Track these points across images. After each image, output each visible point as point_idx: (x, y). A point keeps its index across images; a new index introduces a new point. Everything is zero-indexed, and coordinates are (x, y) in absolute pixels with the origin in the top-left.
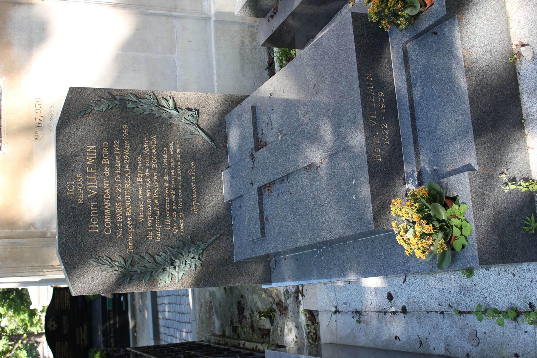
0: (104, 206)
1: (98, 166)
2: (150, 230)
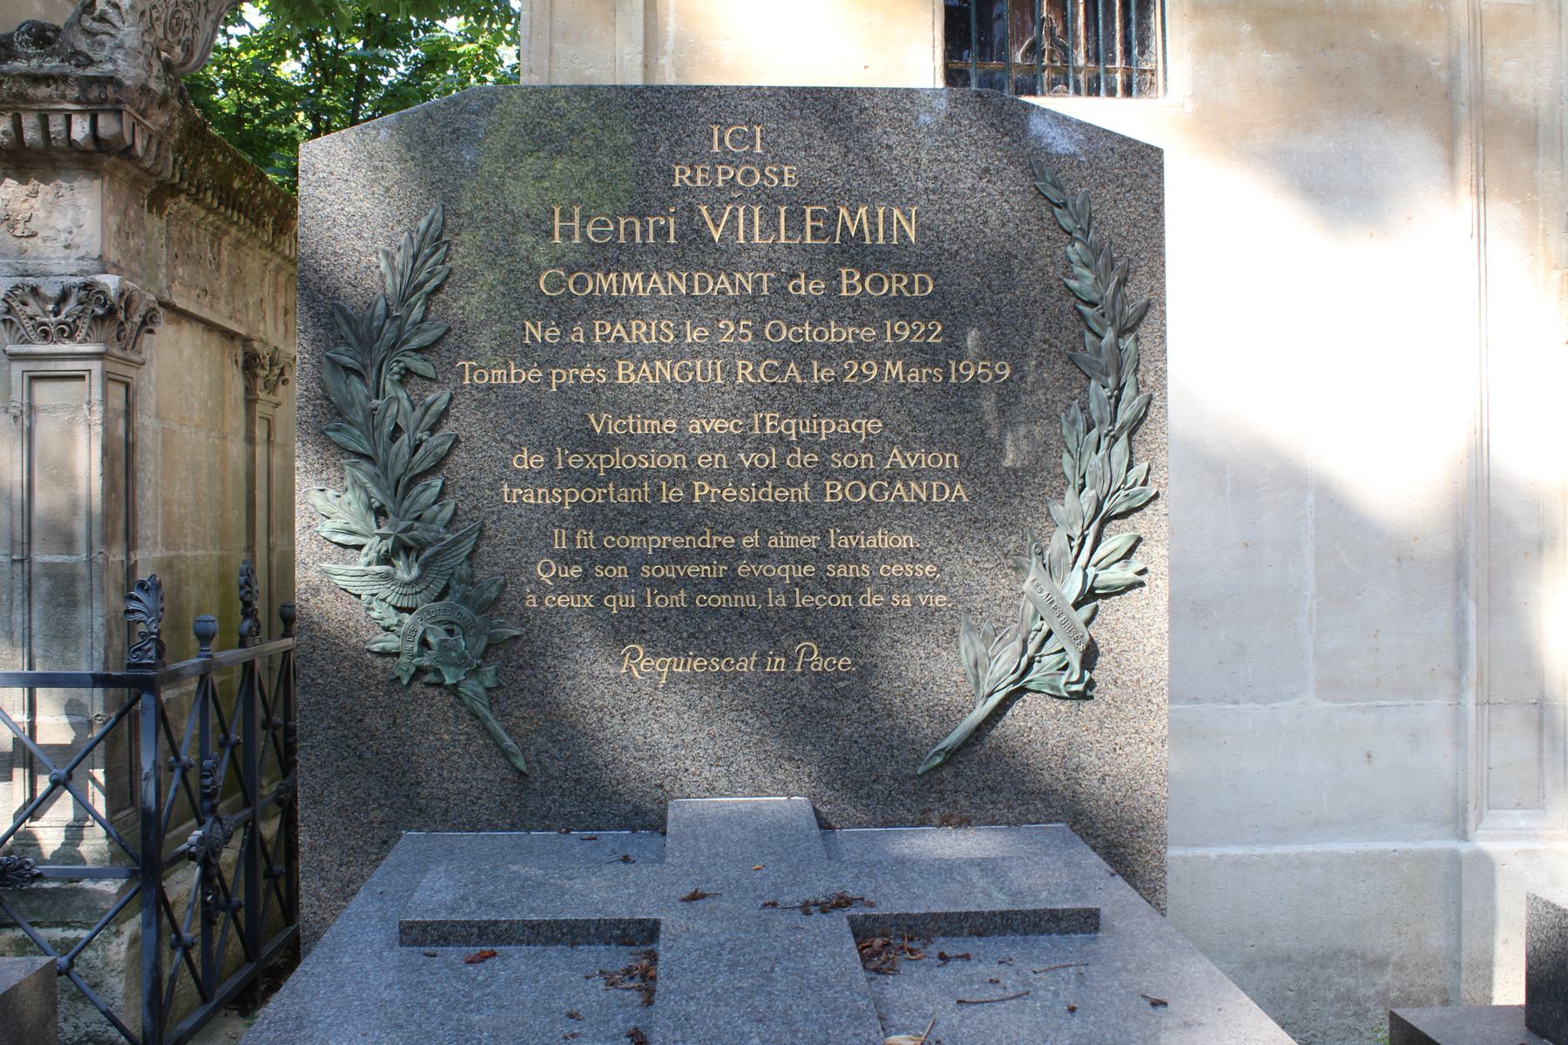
0: (660, 271)
1: (829, 251)
2: (551, 462)
